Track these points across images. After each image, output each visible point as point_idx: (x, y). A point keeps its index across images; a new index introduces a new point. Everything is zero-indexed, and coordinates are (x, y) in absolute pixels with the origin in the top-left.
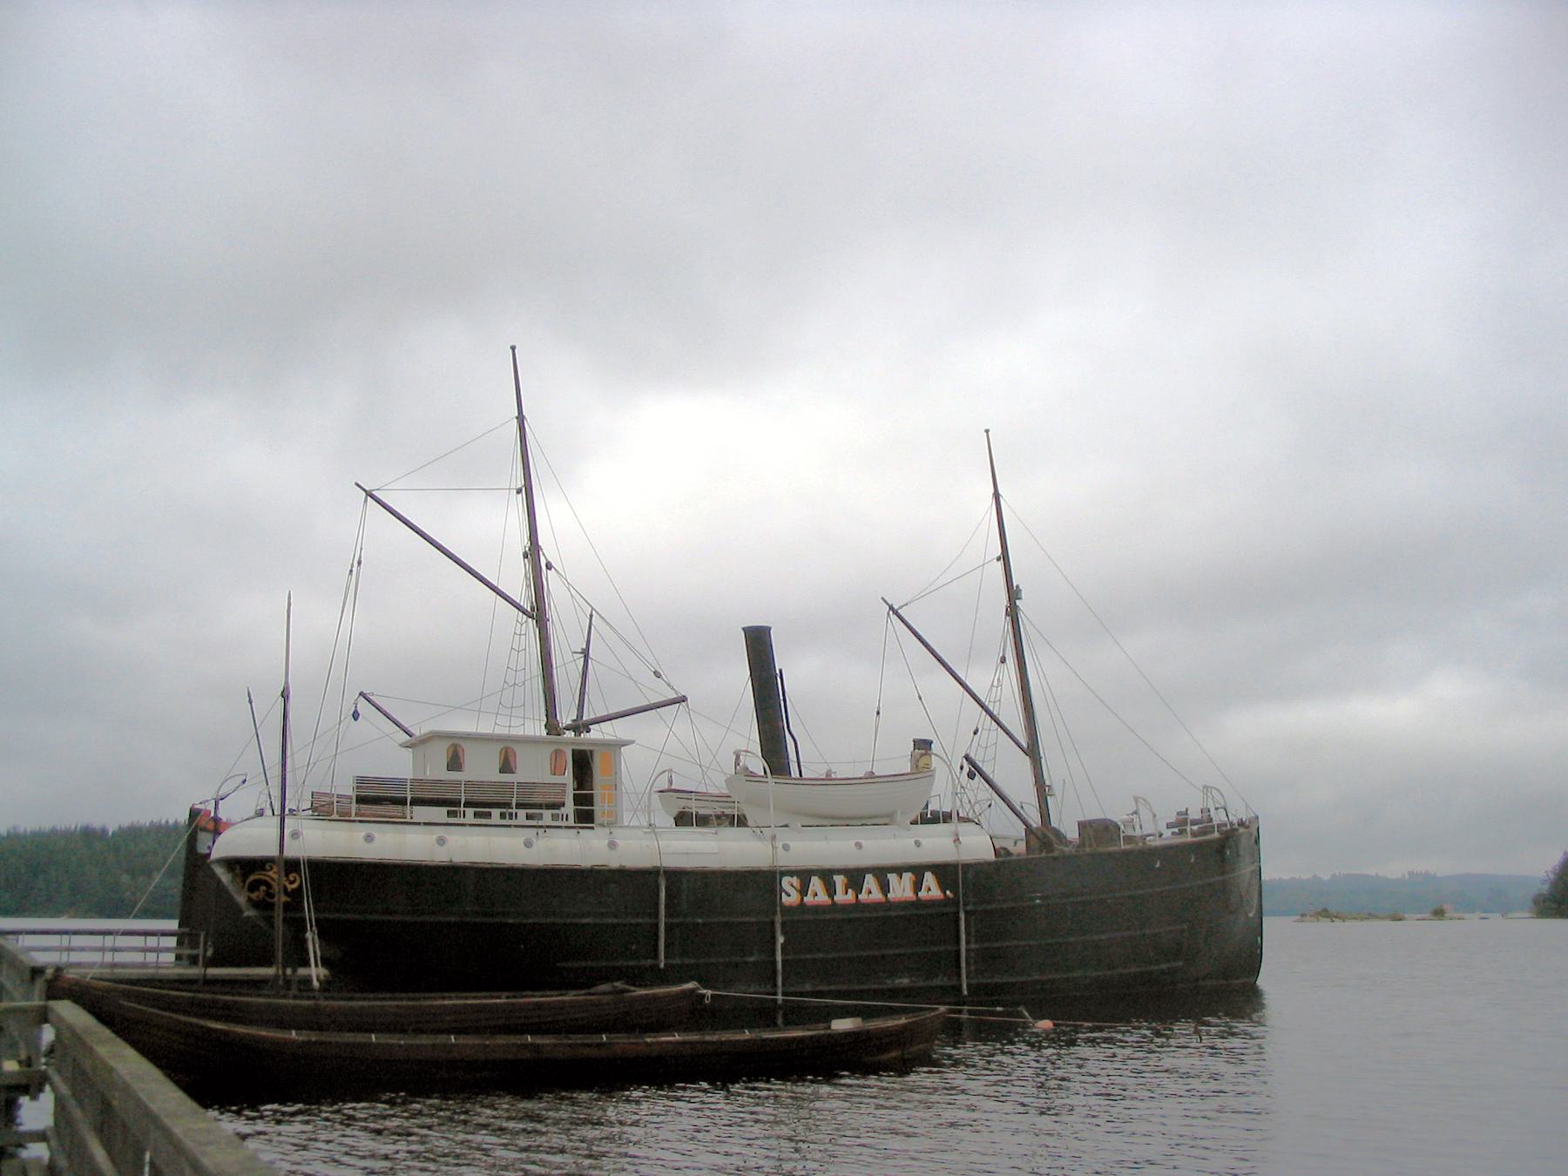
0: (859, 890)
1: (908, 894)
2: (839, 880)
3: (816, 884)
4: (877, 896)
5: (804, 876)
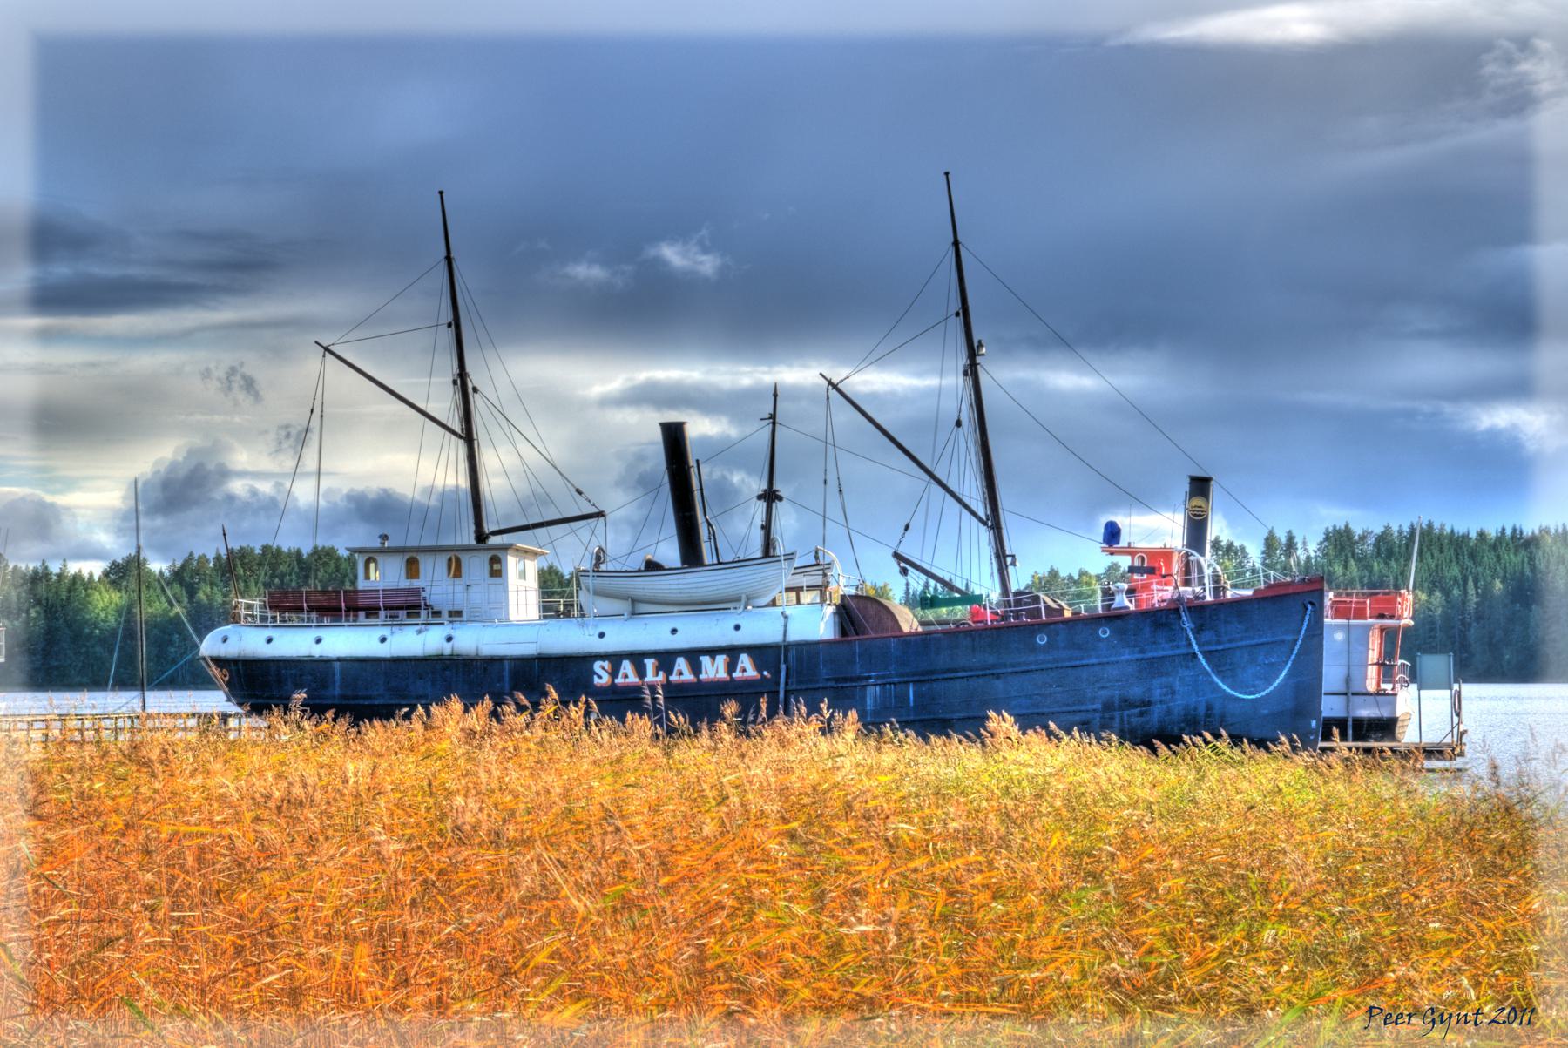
0: (669, 672)
1: (722, 674)
2: (650, 663)
3: (627, 666)
4: (688, 676)
5: (615, 659)
